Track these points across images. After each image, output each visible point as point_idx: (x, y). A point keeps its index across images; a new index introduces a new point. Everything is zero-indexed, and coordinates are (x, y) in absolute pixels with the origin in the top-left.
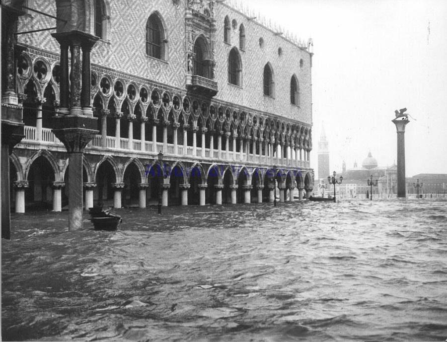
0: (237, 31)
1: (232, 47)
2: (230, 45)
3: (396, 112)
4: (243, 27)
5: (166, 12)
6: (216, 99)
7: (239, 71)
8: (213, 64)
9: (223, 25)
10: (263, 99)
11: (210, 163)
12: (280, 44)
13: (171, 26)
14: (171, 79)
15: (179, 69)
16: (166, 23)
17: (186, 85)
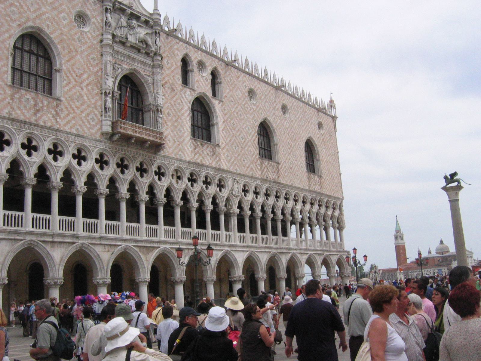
0: (207, 74)
1: (196, 93)
2: (194, 90)
3: (446, 178)
4: (218, 71)
5: (60, 32)
6: (165, 157)
7: (213, 125)
8: (158, 110)
9: (180, 64)
10: (259, 162)
11: (155, 245)
12: (284, 100)
13: (69, 52)
14: (68, 123)
15: (86, 109)
16: (59, 46)
17: (102, 134)
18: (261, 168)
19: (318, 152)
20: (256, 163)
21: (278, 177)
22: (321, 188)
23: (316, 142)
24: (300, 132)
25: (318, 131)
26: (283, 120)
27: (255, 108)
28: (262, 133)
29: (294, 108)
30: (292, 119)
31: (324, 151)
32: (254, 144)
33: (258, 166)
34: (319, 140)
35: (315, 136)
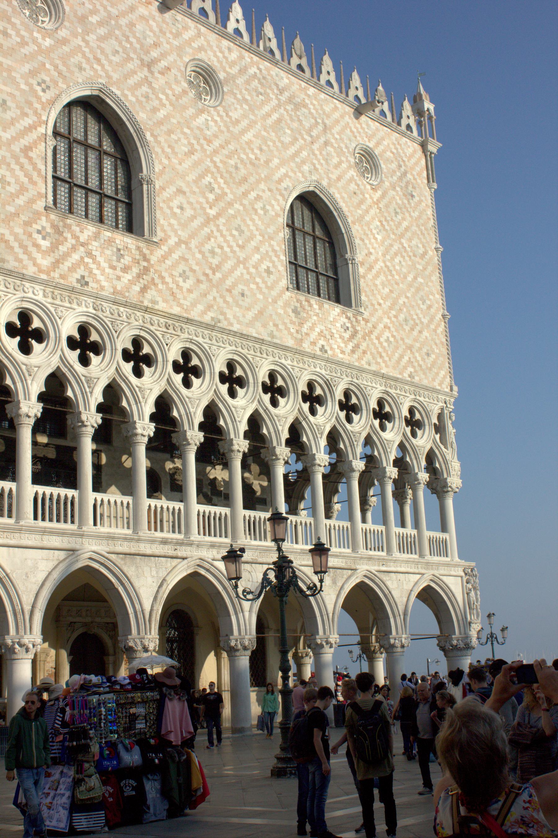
18: (54, 247)
19: (350, 237)
20: (28, 224)
21: (144, 290)
22: (353, 352)
23: (342, 204)
24: (267, 162)
25: (352, 173)
26: (191, 111)
27: (48, 42)
28: (93, 140)
29: (248, 82)
30: (235, 115)
31: (379, 237)
32: (23, 160)
33: (38, 237)
34: (356, 200)
35: (340, 184)
